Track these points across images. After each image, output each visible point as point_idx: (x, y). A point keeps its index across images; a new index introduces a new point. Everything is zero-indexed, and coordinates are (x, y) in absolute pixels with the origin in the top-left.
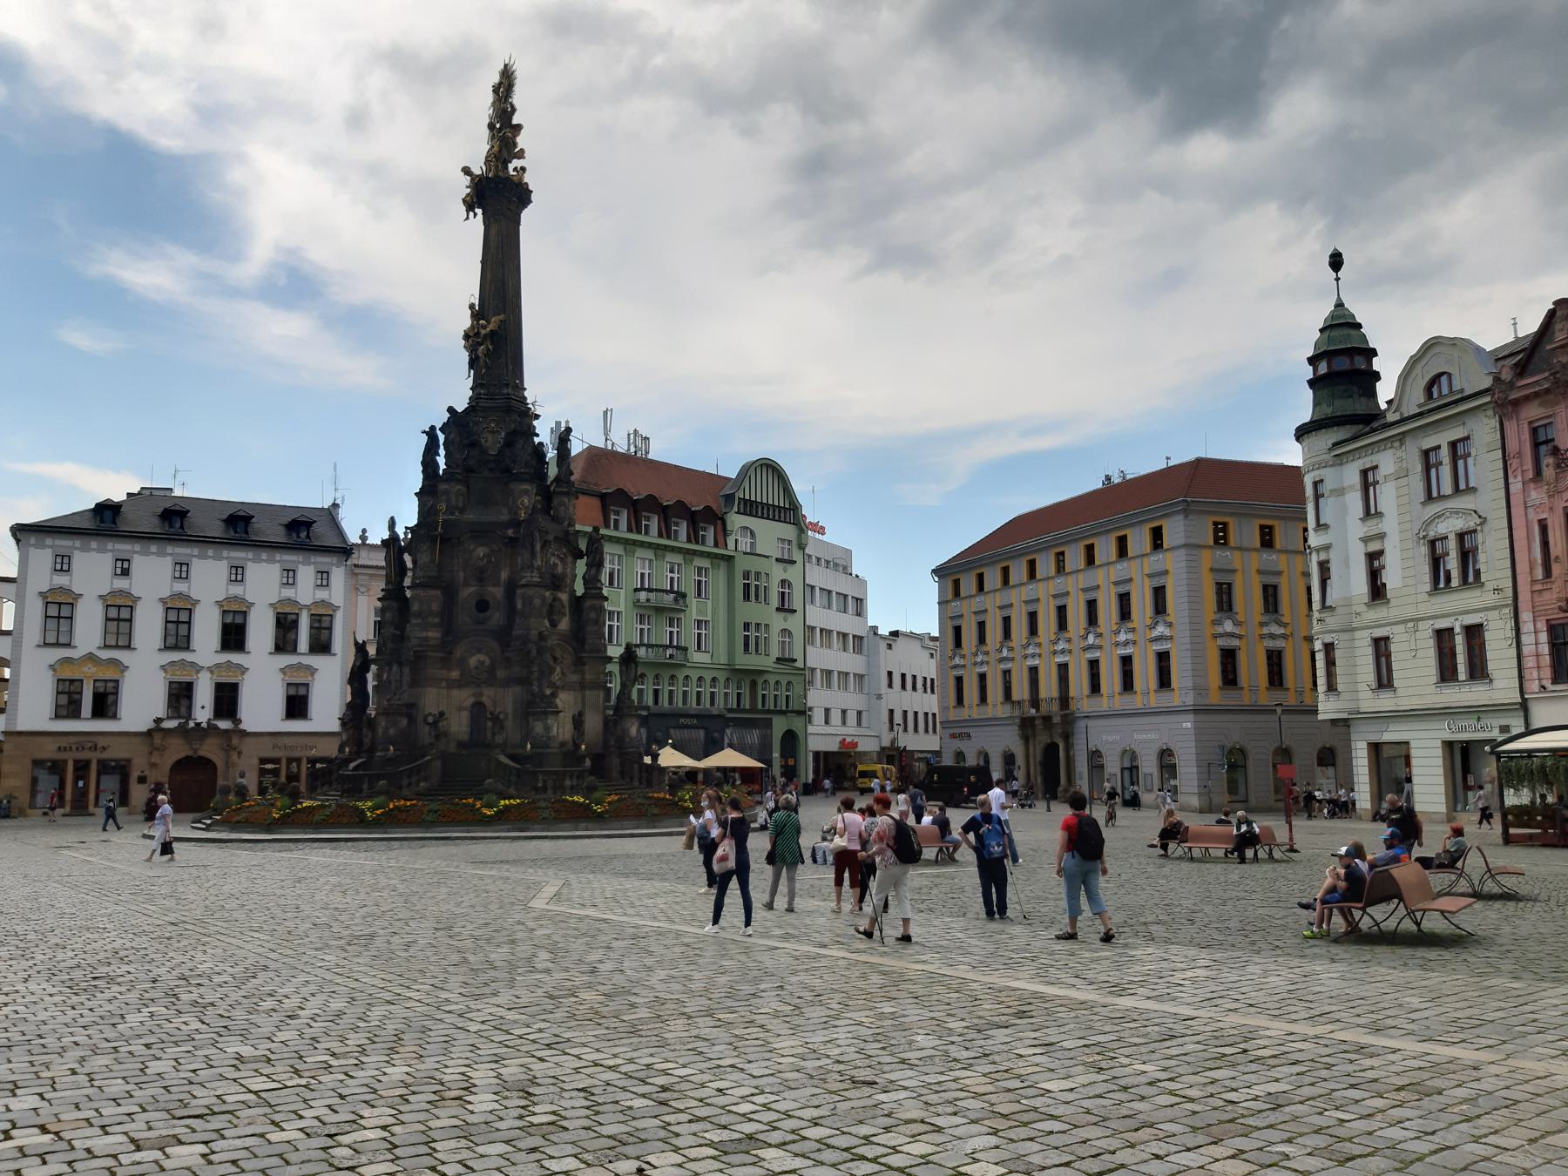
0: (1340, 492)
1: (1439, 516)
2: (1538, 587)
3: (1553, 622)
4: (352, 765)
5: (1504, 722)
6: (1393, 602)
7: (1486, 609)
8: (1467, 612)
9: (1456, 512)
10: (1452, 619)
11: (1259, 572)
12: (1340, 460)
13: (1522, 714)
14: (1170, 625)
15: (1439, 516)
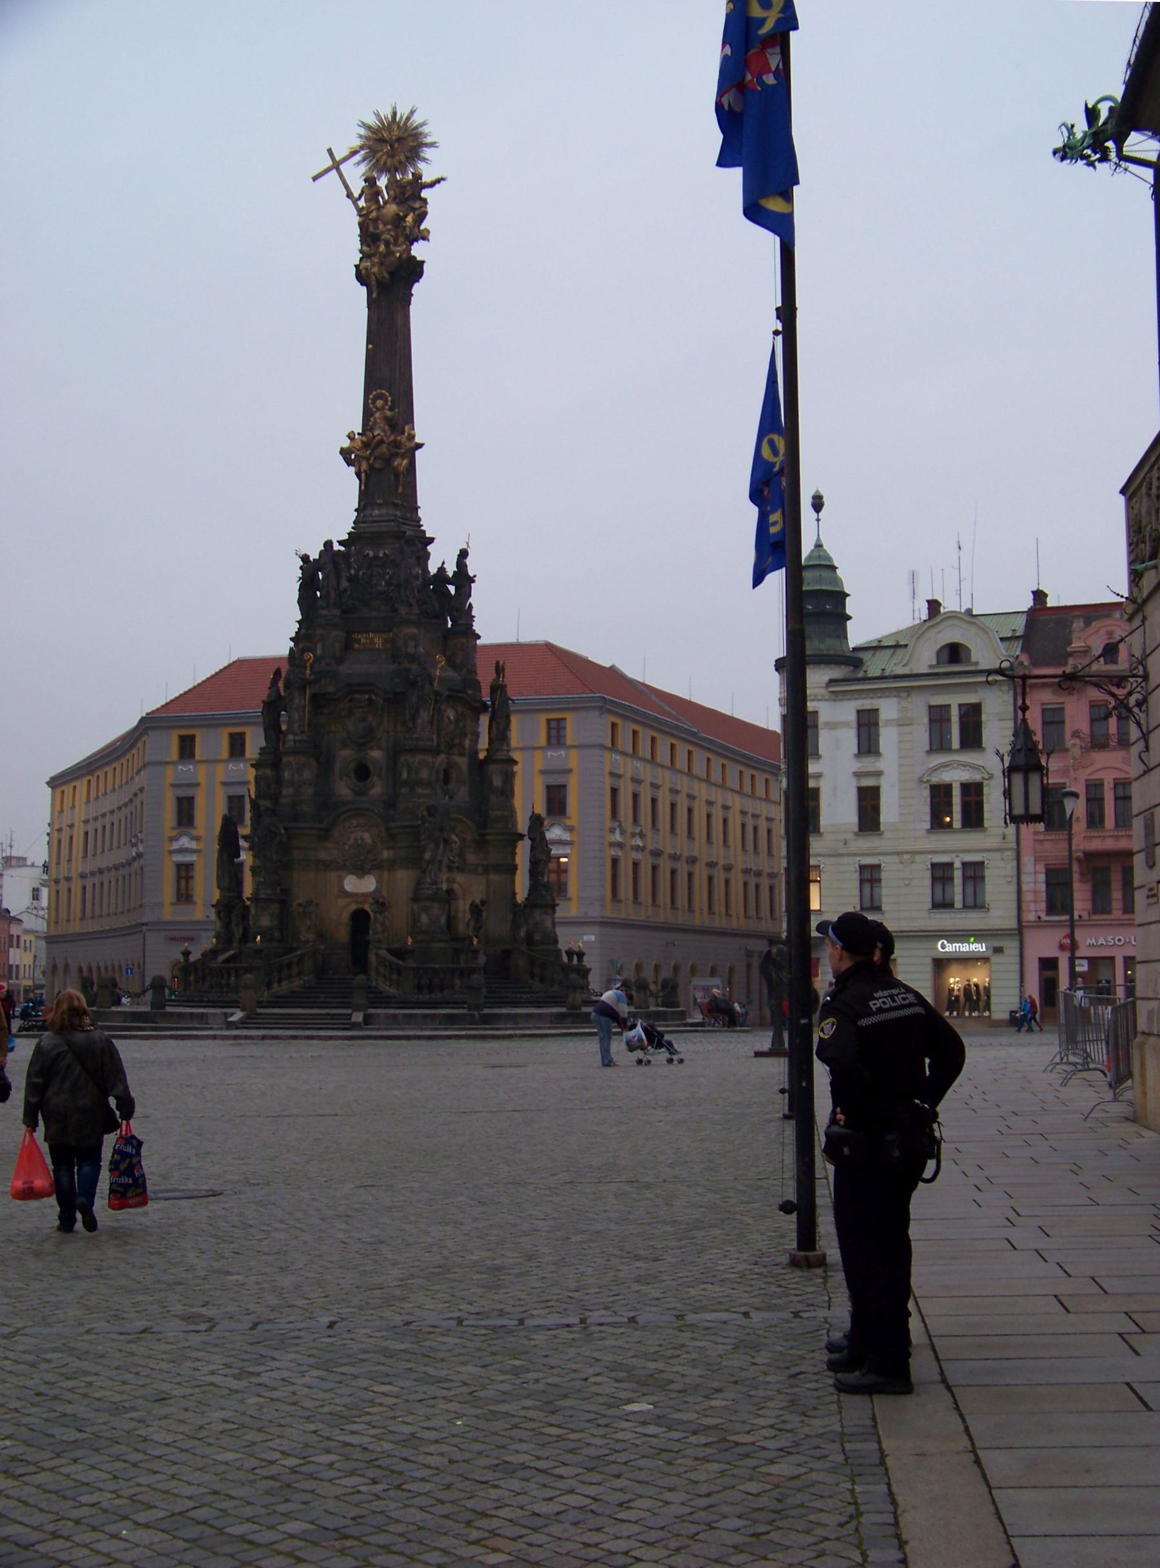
0: (832, 726)
1: (945, 766)
2: (1041, 837)
3: (1049, 867)
4: (222, 958)
5: (997, 944)
6: (887, 835)
7: (989, 850)
8: (969, 851)
9: (965, 765)
10: (953, 856)
11: (544, 772)
12: (836, 696)
13: (1017, 938)
14: (570, 829)
15: (945, 766)
